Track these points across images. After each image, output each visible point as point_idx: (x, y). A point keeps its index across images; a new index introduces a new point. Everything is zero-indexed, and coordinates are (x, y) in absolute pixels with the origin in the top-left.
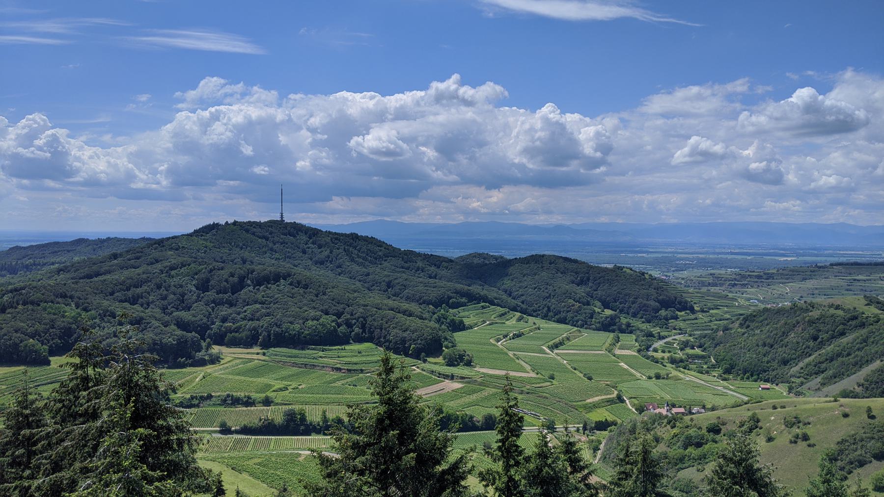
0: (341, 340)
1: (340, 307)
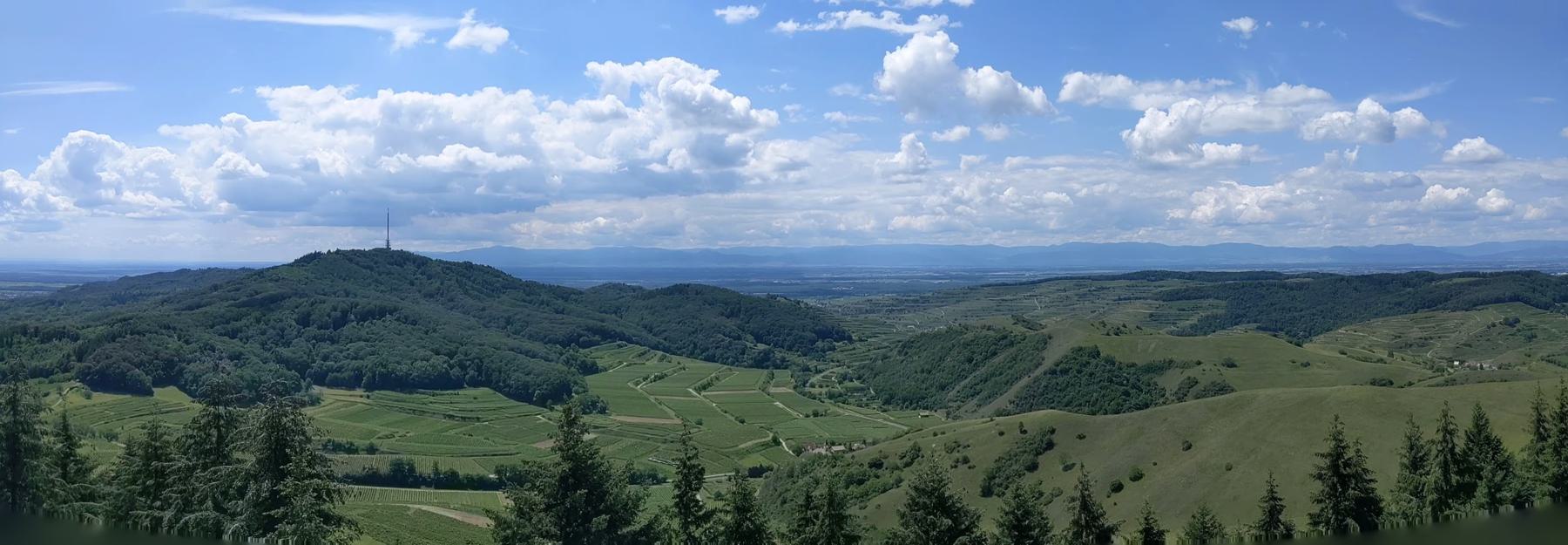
0: (457, 384)
1: (453, 347)
